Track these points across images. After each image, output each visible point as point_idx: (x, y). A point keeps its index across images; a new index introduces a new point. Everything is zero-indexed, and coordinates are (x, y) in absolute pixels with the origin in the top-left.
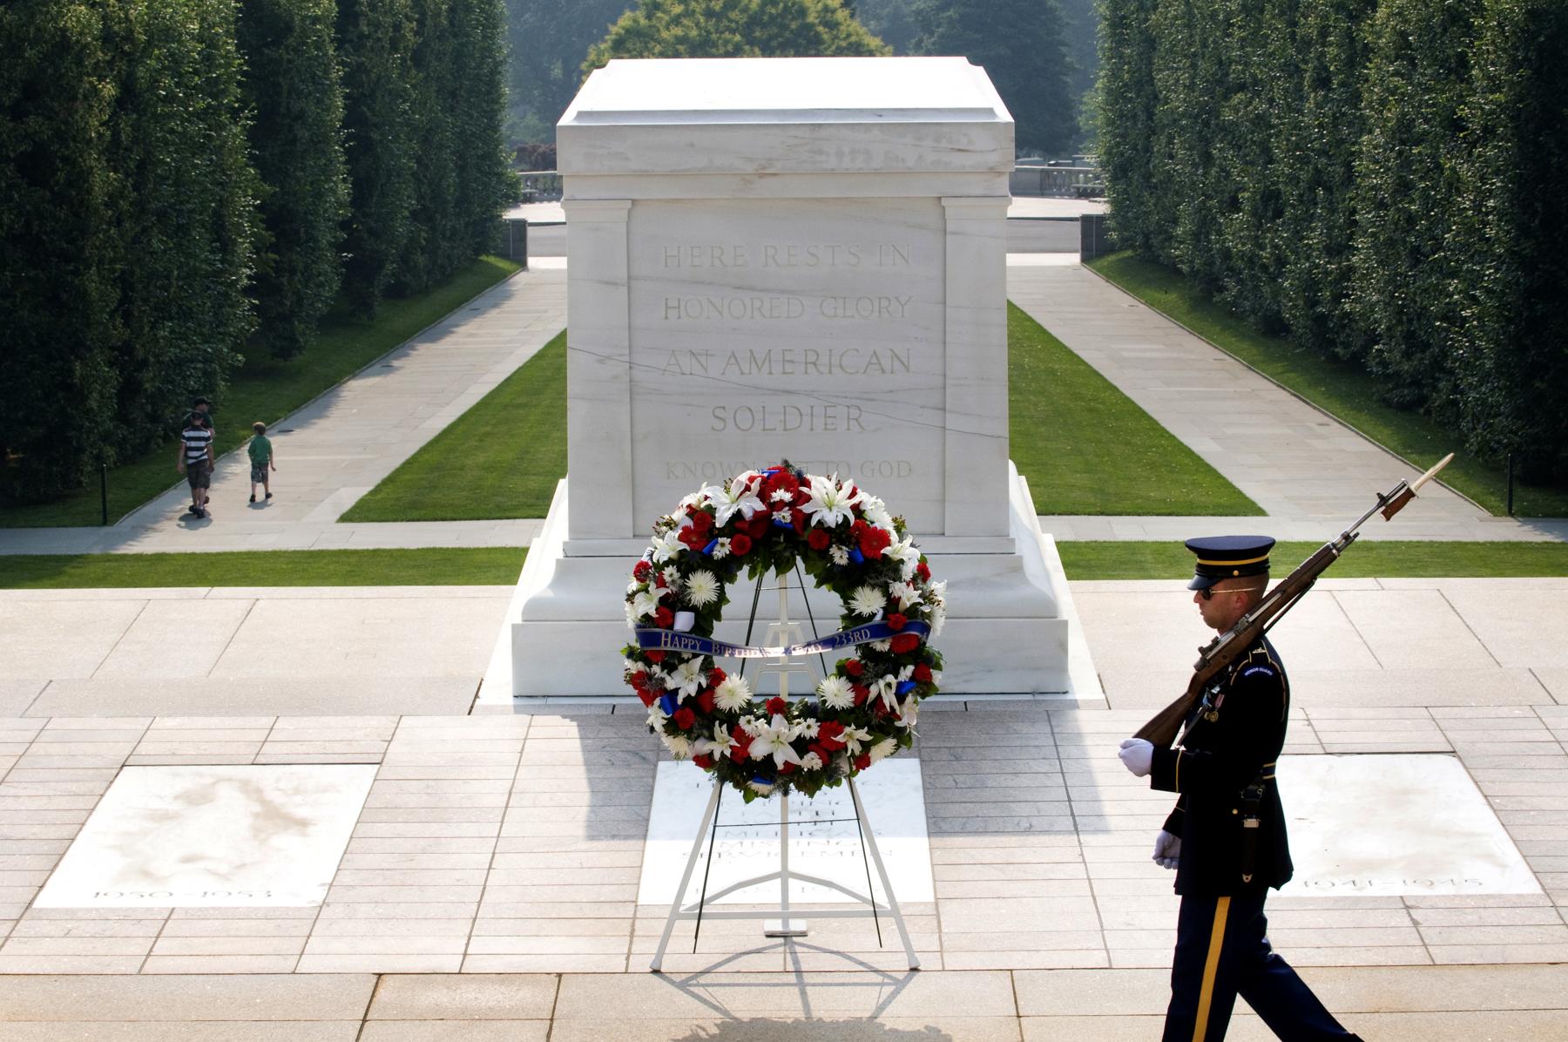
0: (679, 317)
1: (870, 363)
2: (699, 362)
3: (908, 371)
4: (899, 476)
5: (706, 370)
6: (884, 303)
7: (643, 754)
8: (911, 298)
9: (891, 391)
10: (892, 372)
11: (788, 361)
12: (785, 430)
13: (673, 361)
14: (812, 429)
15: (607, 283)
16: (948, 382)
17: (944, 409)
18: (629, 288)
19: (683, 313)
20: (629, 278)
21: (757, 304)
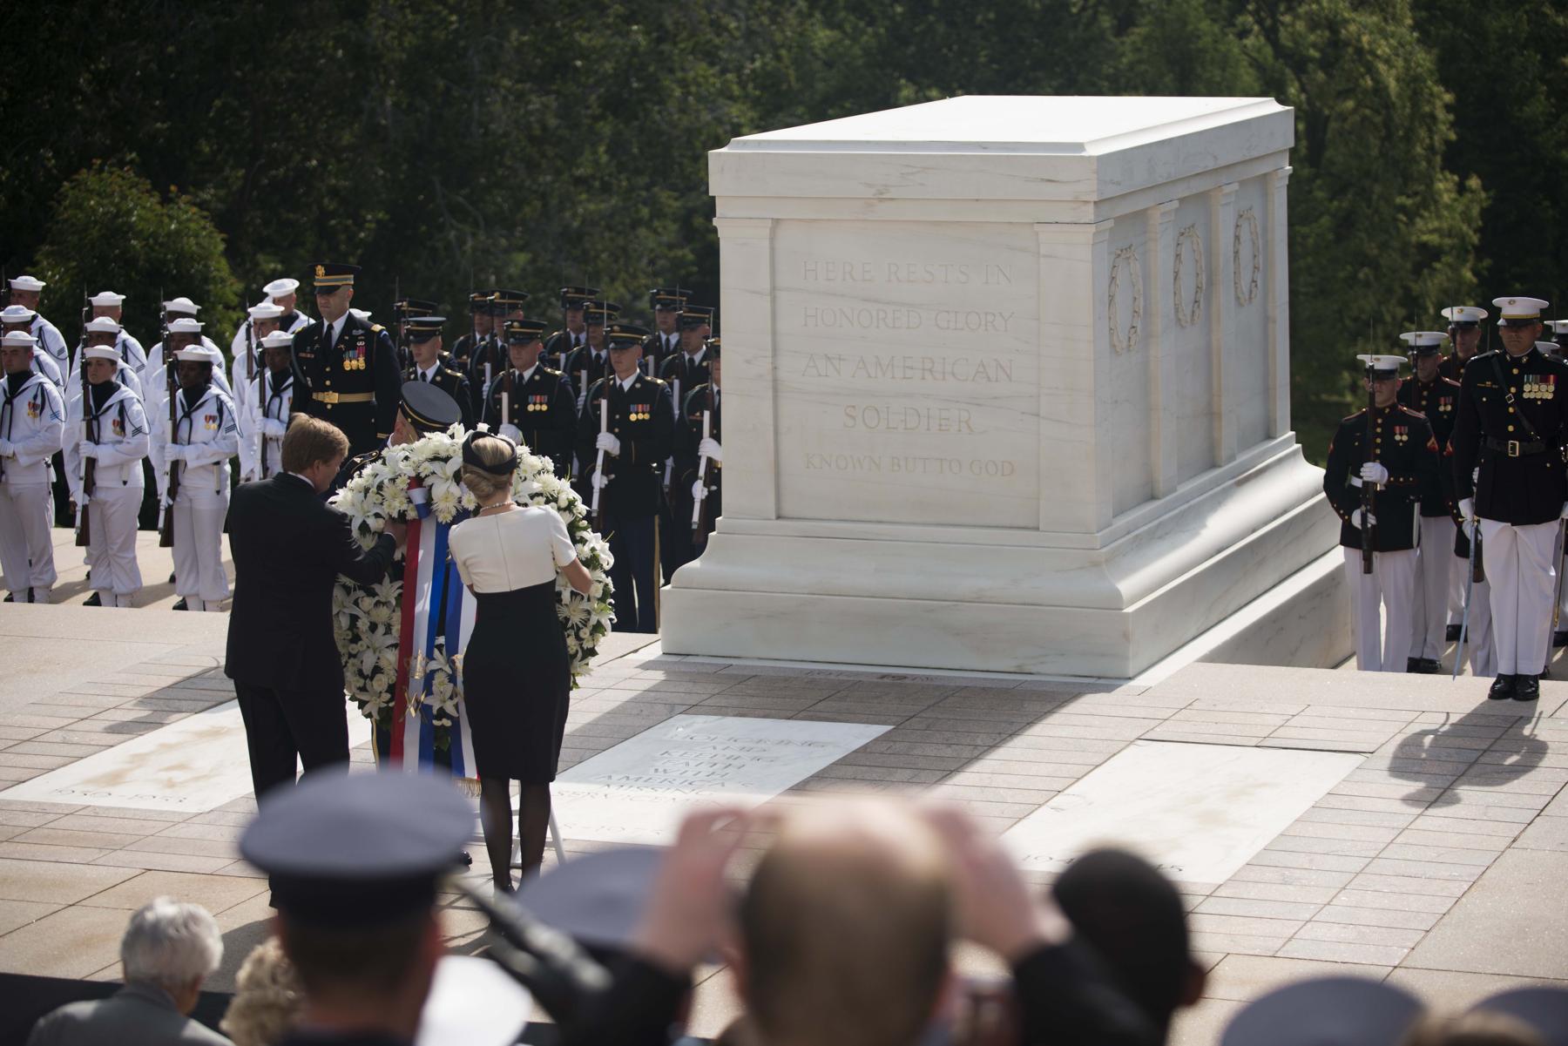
0: (817, 325)
1: (978, 372)
2: (832, 363)
3: (1010, 380)
5: (839, 373)
6: (990, 318)
9: (996, 398)
10: (997, 381)
11: (907, 367)
12: (906, 429)
14: (928, 429)
15: (754, 292)
17: (1038, 415)
18: (774, 300)
20: (774, 289)
21: (882, 315)
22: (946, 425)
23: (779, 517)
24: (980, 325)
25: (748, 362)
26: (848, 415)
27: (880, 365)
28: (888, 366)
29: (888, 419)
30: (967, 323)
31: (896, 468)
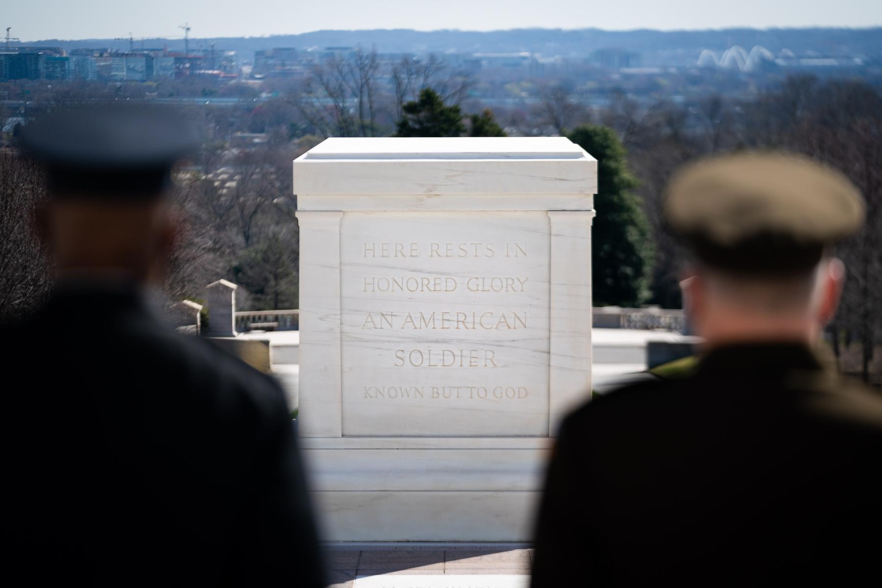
1: (500, 322)
2: (386, 319)
3: (525, 327)
4: (519, 397)
5: (391, 326)
7: (347, 572)
8: (527, 278)
9: (514, 341)
12: (443, 366)
13: (369, 320)
16: (553, 334)
17: (549, 353)
18: (341, 270)
19: (376, 288)
20: (341, 264)
22: (475, 362)
23: (343, 436)
24: (502, 287)
25: (321, 319)
26: (398, 357)
27: (424, 318)
28: (430, 319)
29: (429, 359)
30: (492, 286)
31: (436, 395)
